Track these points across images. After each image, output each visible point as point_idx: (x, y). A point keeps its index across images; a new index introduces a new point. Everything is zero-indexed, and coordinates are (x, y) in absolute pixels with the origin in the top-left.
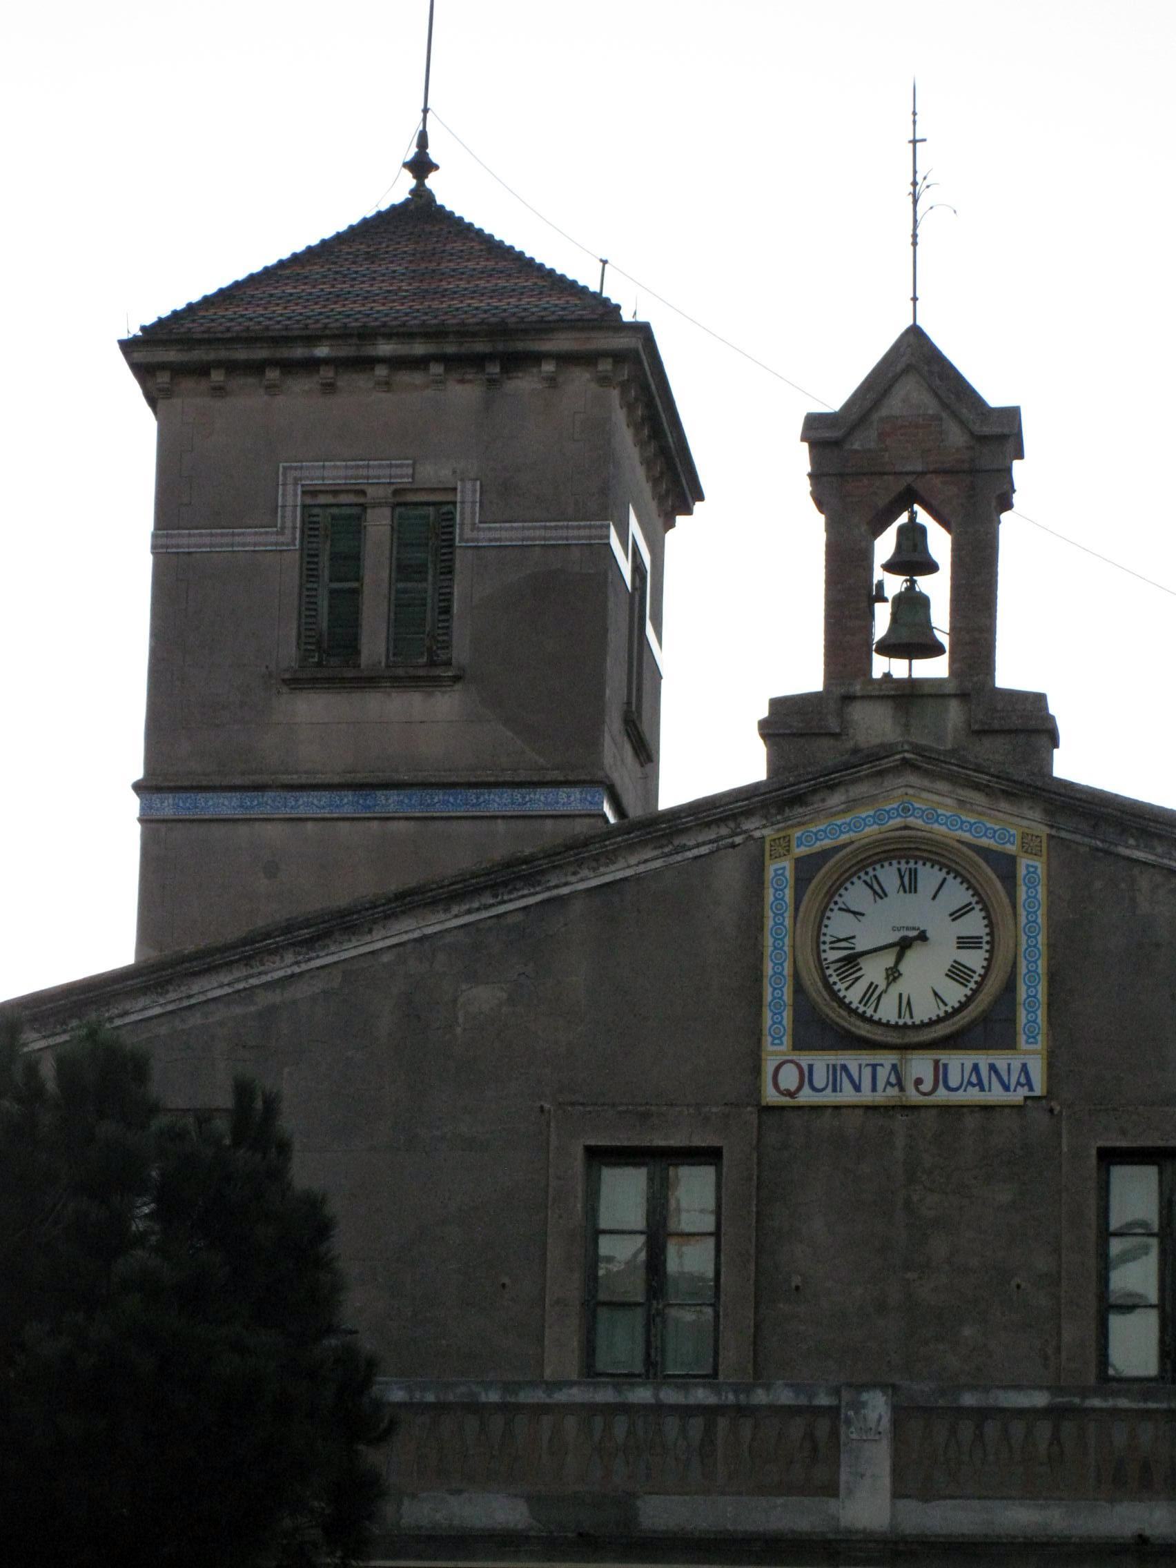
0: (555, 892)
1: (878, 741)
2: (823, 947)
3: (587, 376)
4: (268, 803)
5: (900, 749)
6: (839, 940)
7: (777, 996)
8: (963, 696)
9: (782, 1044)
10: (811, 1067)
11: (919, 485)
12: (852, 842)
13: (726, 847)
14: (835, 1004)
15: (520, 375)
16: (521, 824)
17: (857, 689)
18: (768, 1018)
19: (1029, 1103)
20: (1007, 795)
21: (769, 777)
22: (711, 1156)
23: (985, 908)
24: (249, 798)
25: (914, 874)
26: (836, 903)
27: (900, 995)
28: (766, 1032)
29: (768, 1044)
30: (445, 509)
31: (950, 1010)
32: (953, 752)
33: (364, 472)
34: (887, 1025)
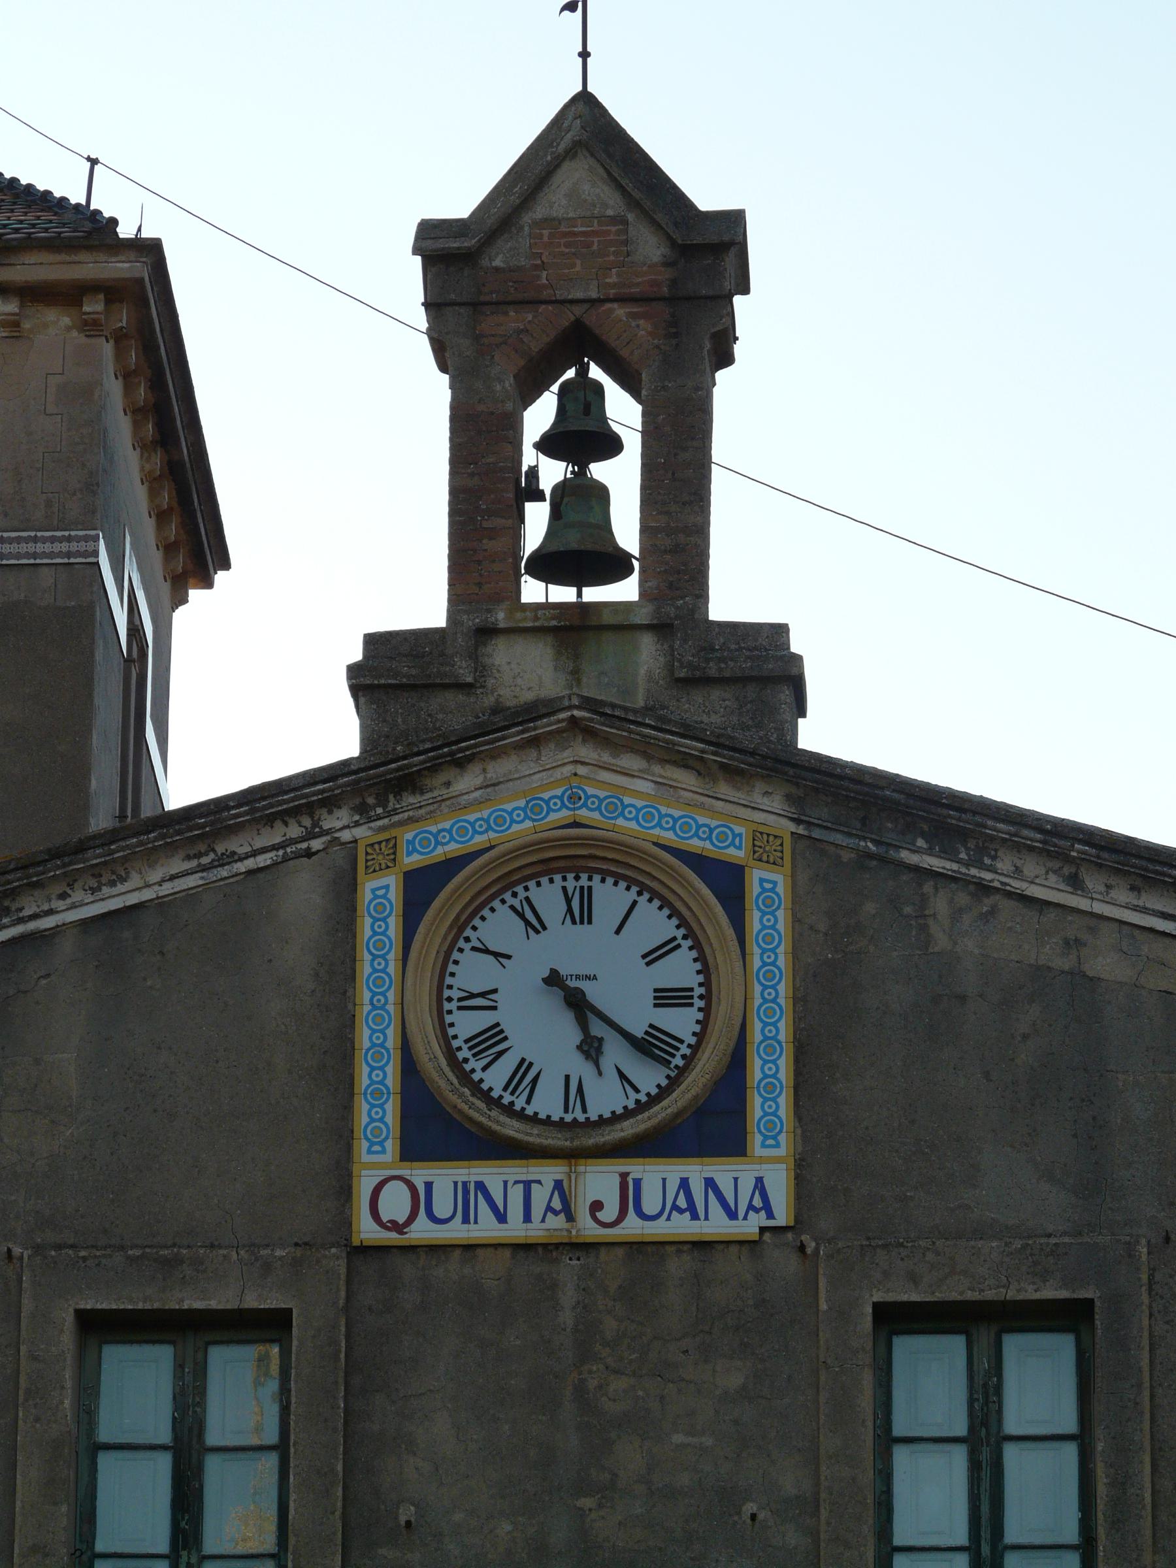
0: (32, 926)
1: (529, 696)
2: (447, 1006)
3: (66, 321)
5: (567, 703)
6: (472, 996)
7: (377, 1079)
8: (661, 629)
9: (384, 1151)
10: (429, 1186)
11: (591, 320)
12: (492, 847)
13: (298, 855)
14: (467, 1091)
17: (501, 617)
18: (363, 1112)
19: (767, 1236)
20: (732, 773)
21: (364, 750)
22: (270, 1325)
23: (696, 946)
25: (587, 895)
26: (467, 940)
27: (567, 1078)
28: (358, 1132)
29: (362, 1148)
31: (643, 1098)
32: (648, 710)
34: (548, 1121)
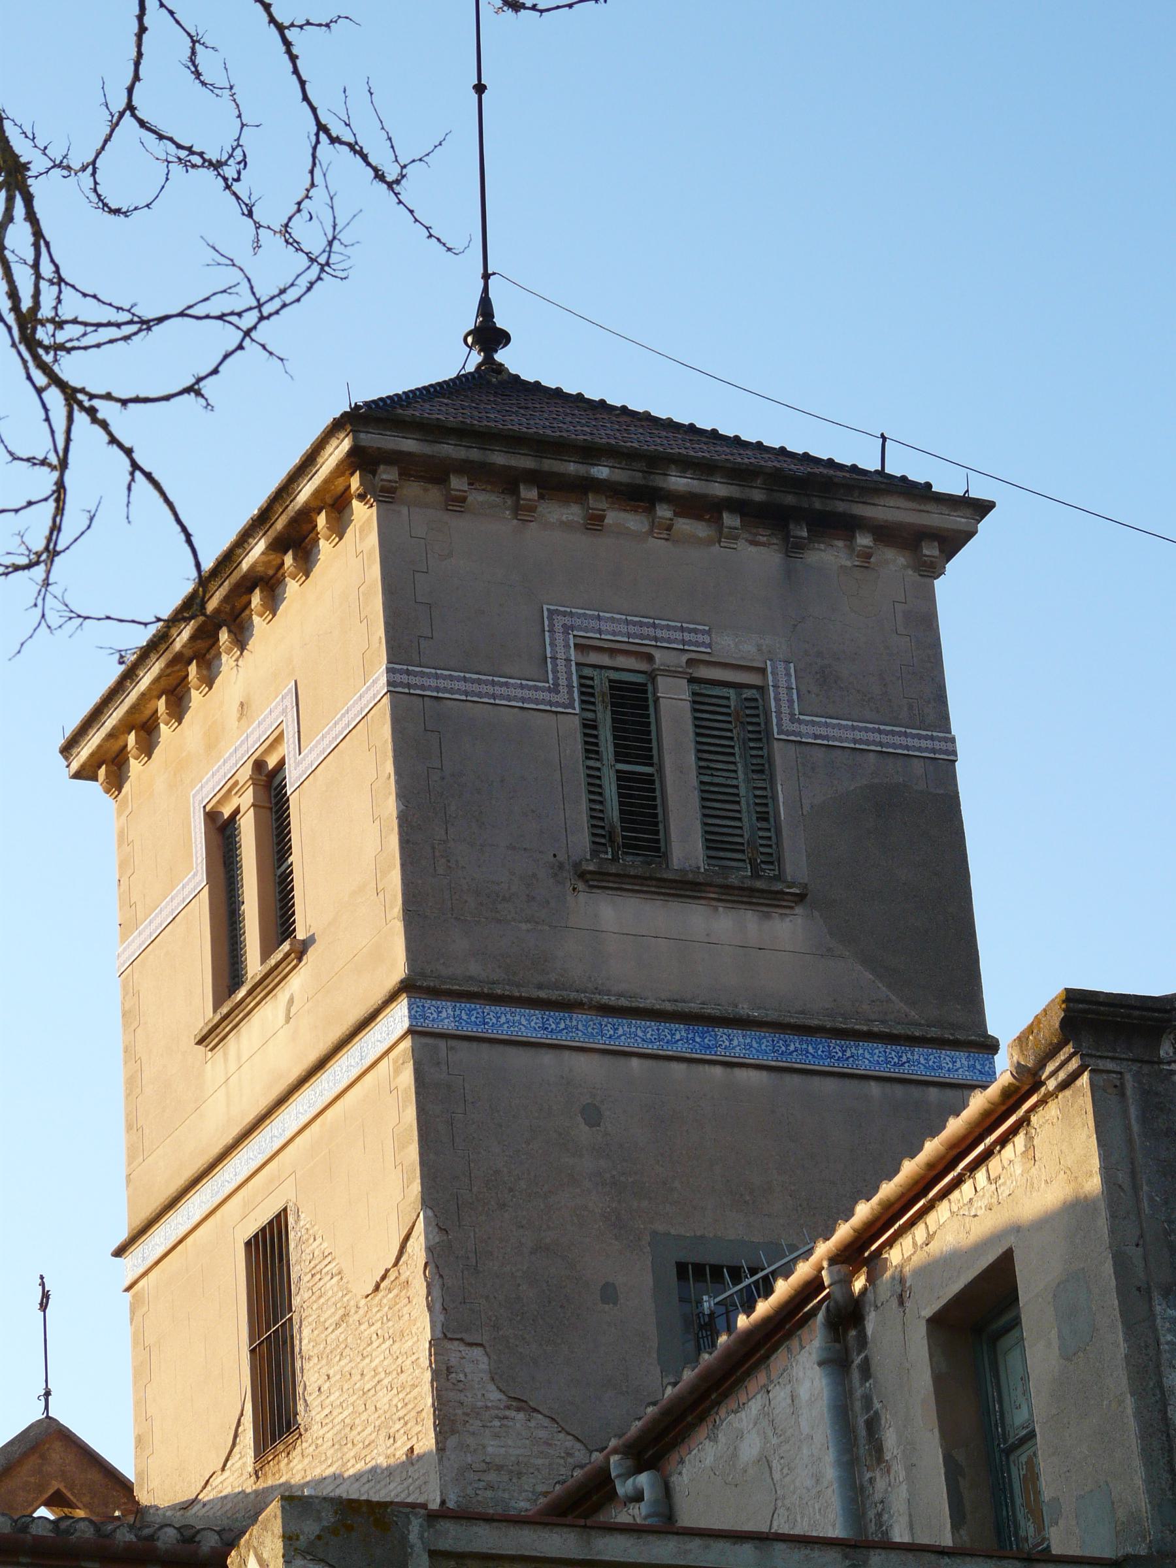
3: (901, 560)
4: (580, 1028)
15: (822, 546)
16: (899, 1090)
24: (556, 1020)
30: (748, 693)
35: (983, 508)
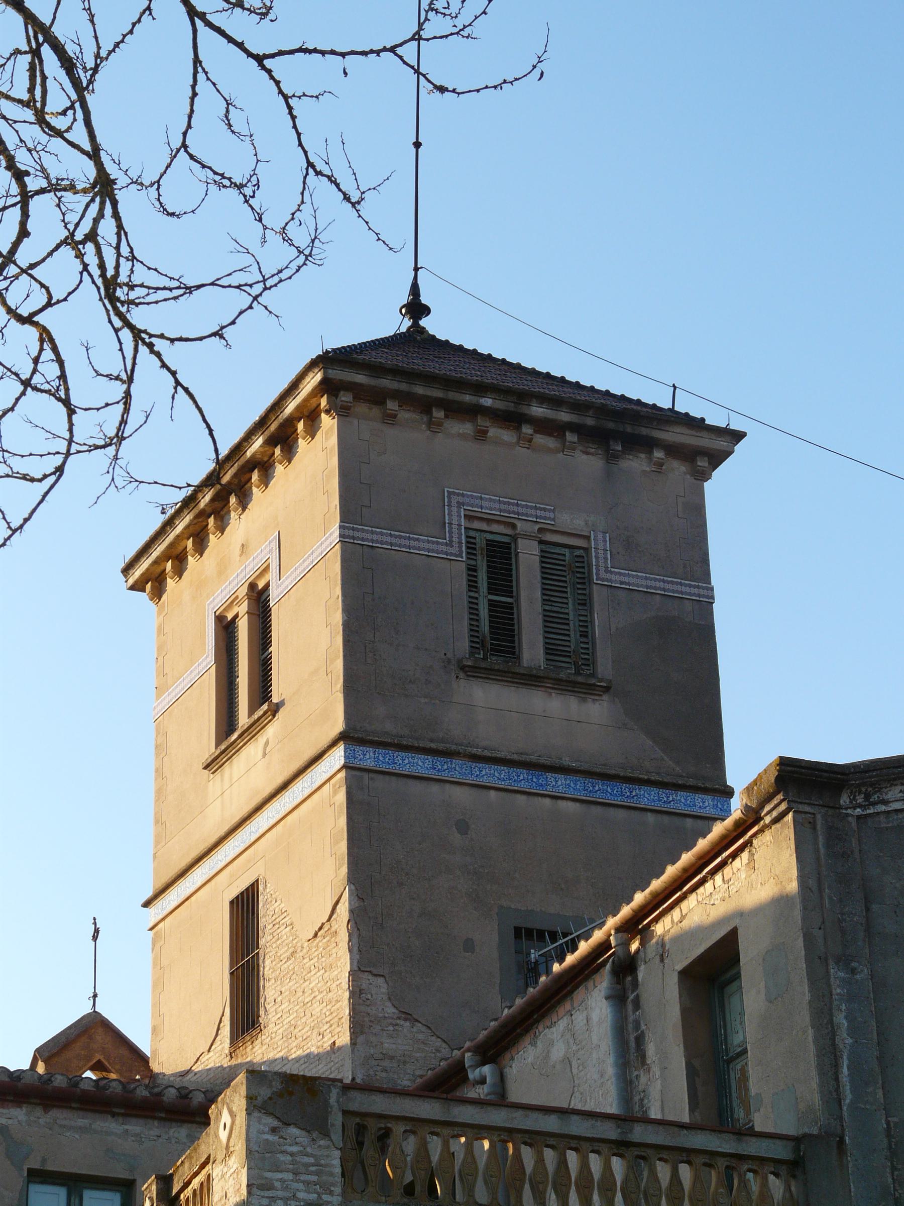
3: (683, 469)
4: (457, 769)
15: (631, 457)
16: (666, 819)
24: (441, 763)
30: (578, 552)
33: (515, 509)
35: (739, 436)
